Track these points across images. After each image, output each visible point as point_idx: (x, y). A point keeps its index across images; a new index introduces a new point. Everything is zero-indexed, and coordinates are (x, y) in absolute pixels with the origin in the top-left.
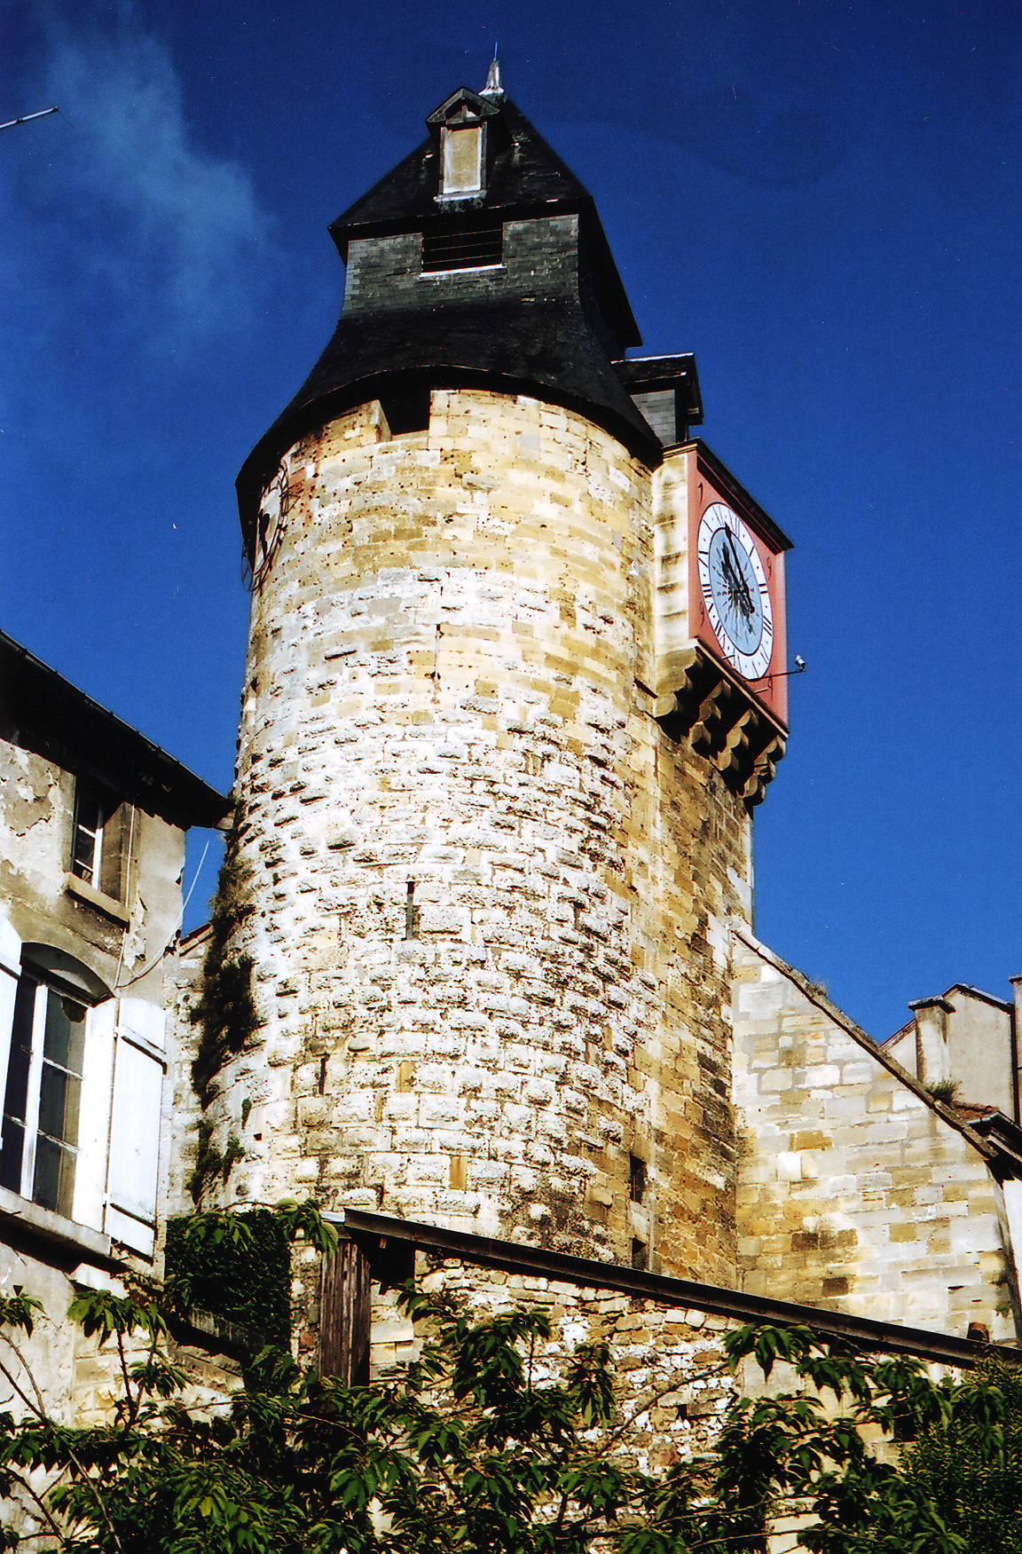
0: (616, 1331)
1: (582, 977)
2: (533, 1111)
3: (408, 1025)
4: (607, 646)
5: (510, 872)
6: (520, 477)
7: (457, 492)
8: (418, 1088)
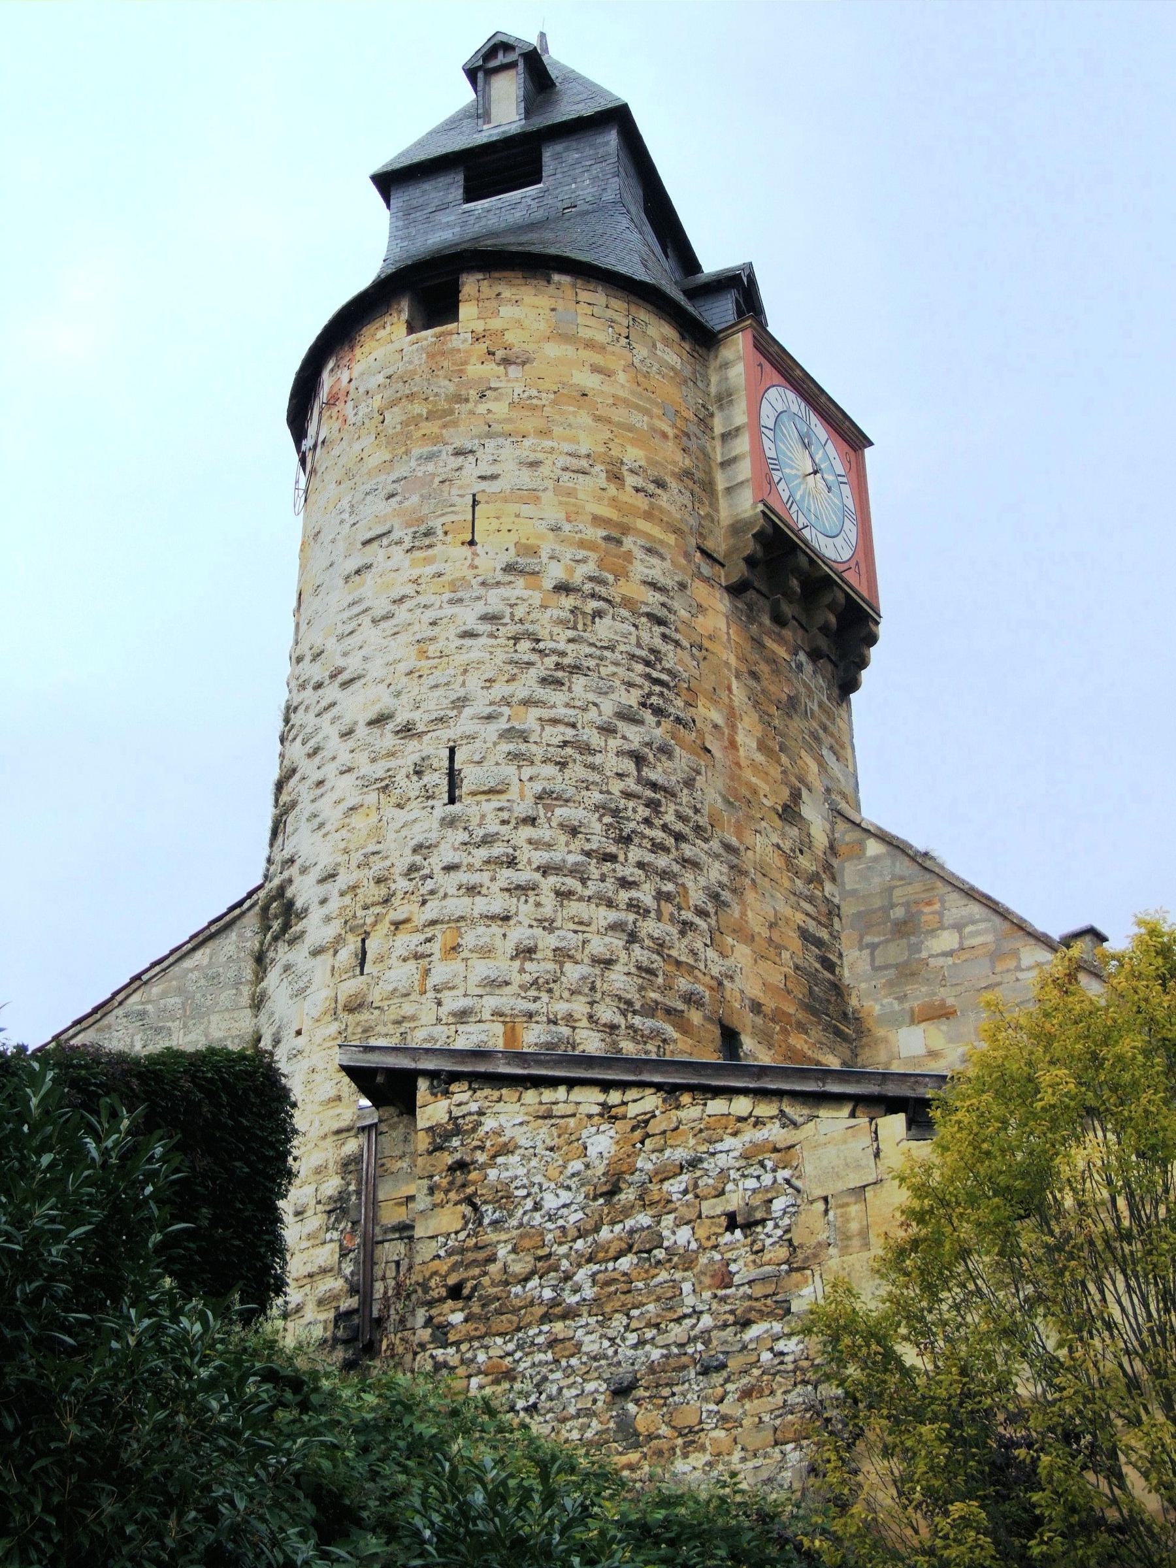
0: (648, 1136)
1: (647, 832)
2: (597, 971)
3: (452, 891)
4: (660, 509)
5: (561, 728)
6: (553, 350)
7: (491, 369)
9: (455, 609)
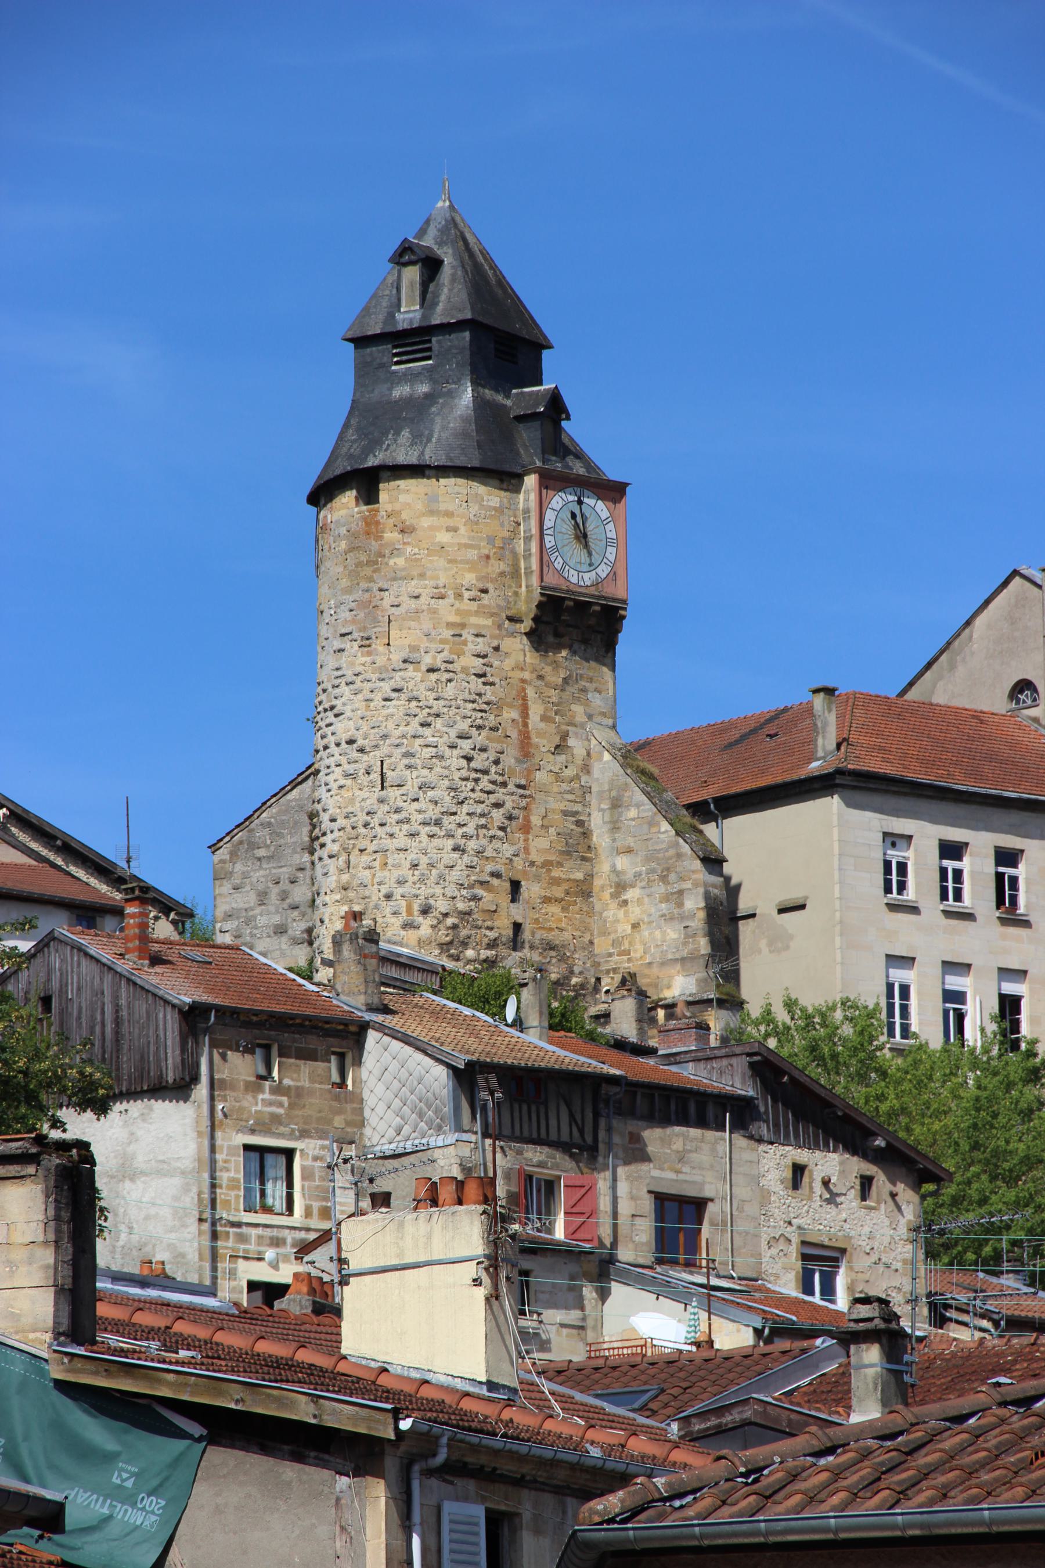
3: (384, 836)
4: (484, 606)
5: (430, 749)
6: (426, 522)
8: (390, 867)
9: (382, 684)
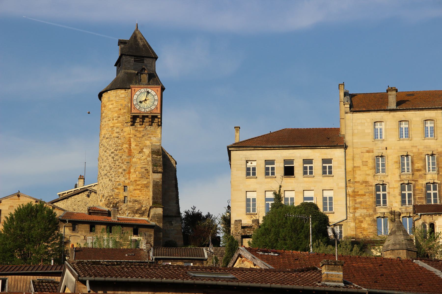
6: (108, 104)
